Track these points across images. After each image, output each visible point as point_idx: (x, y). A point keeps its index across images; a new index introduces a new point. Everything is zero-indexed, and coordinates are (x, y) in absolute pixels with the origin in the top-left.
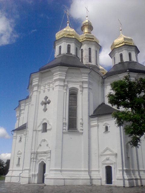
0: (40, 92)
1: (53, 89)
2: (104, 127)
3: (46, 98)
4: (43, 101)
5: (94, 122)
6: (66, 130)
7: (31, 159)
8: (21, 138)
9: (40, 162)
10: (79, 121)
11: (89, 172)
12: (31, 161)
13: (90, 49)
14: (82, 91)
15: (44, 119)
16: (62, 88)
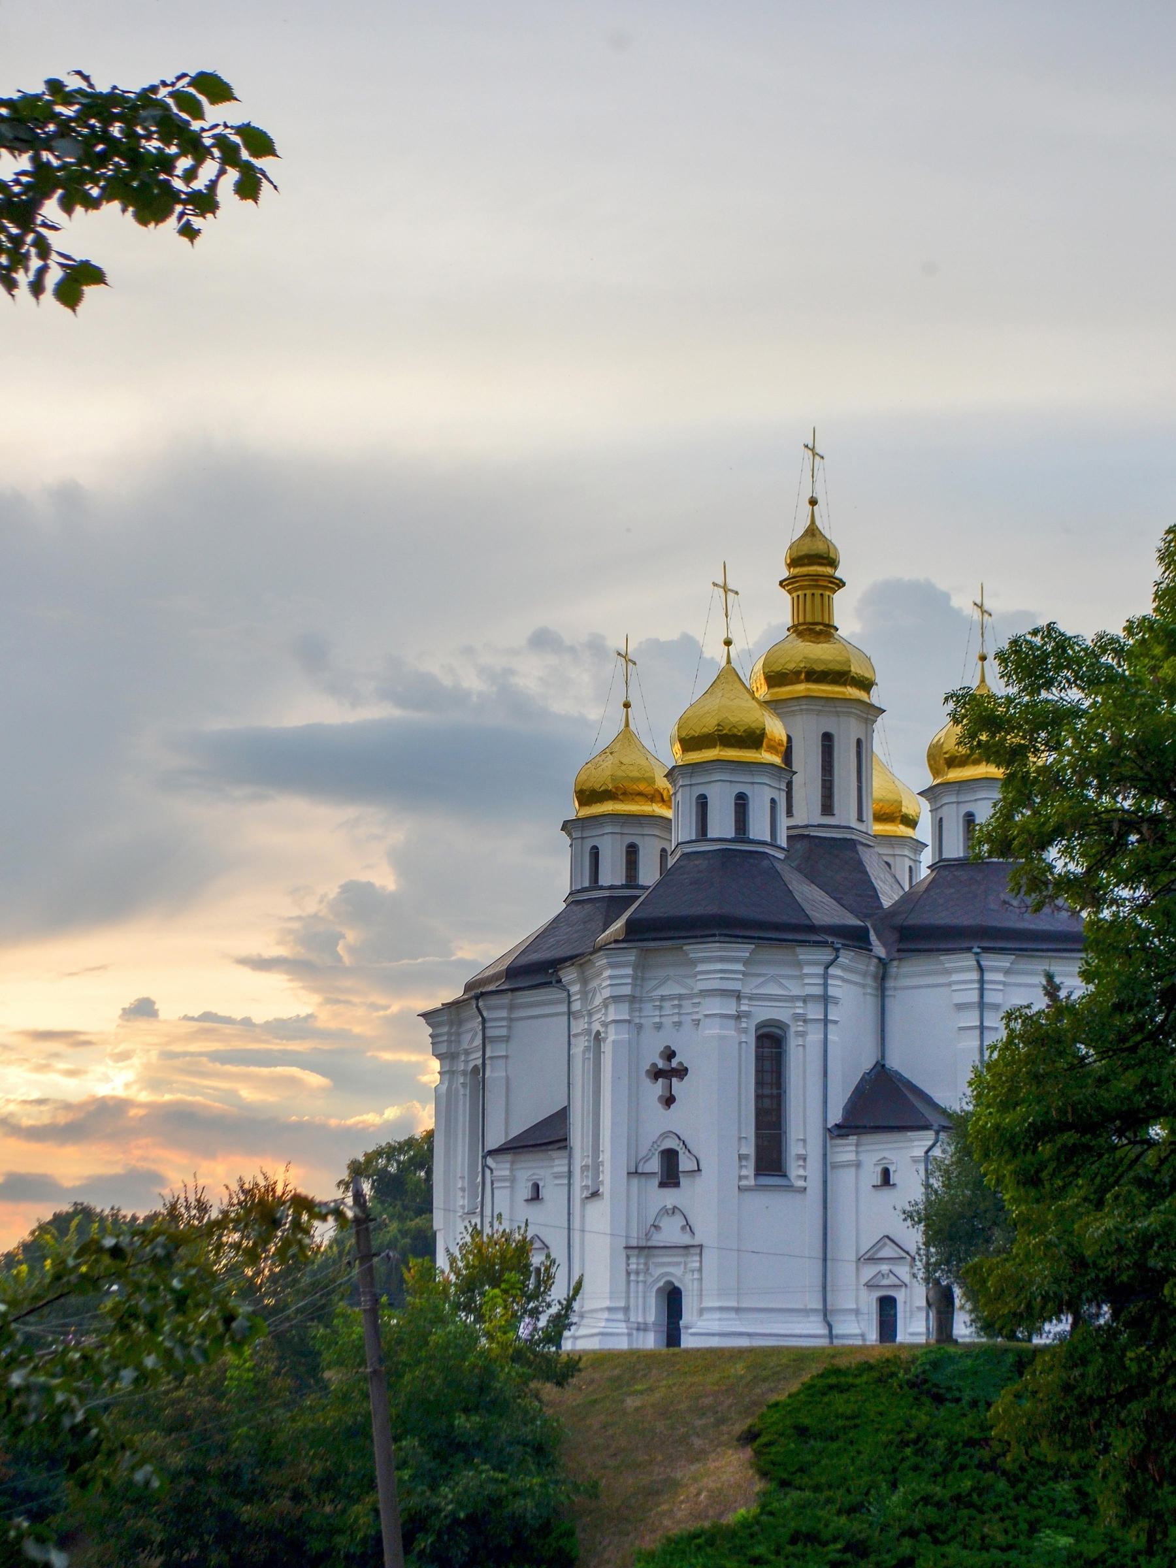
0: (640, 1027)
1: (697, 1023)
2: (879, 1169)
3: (670, 1055)
4: (654, 1065)
5: (846, 1151)
6: (746, 1177)
7: (628, 1273)
8: (536, 1187)
9: (661, 1284)
10: (793, 1149)
11: (826, 1314)
12: (628, 1282)
13: (827, 738)
14: (802, 1034)
15: (666, 1135)
16: (732, 1022)
